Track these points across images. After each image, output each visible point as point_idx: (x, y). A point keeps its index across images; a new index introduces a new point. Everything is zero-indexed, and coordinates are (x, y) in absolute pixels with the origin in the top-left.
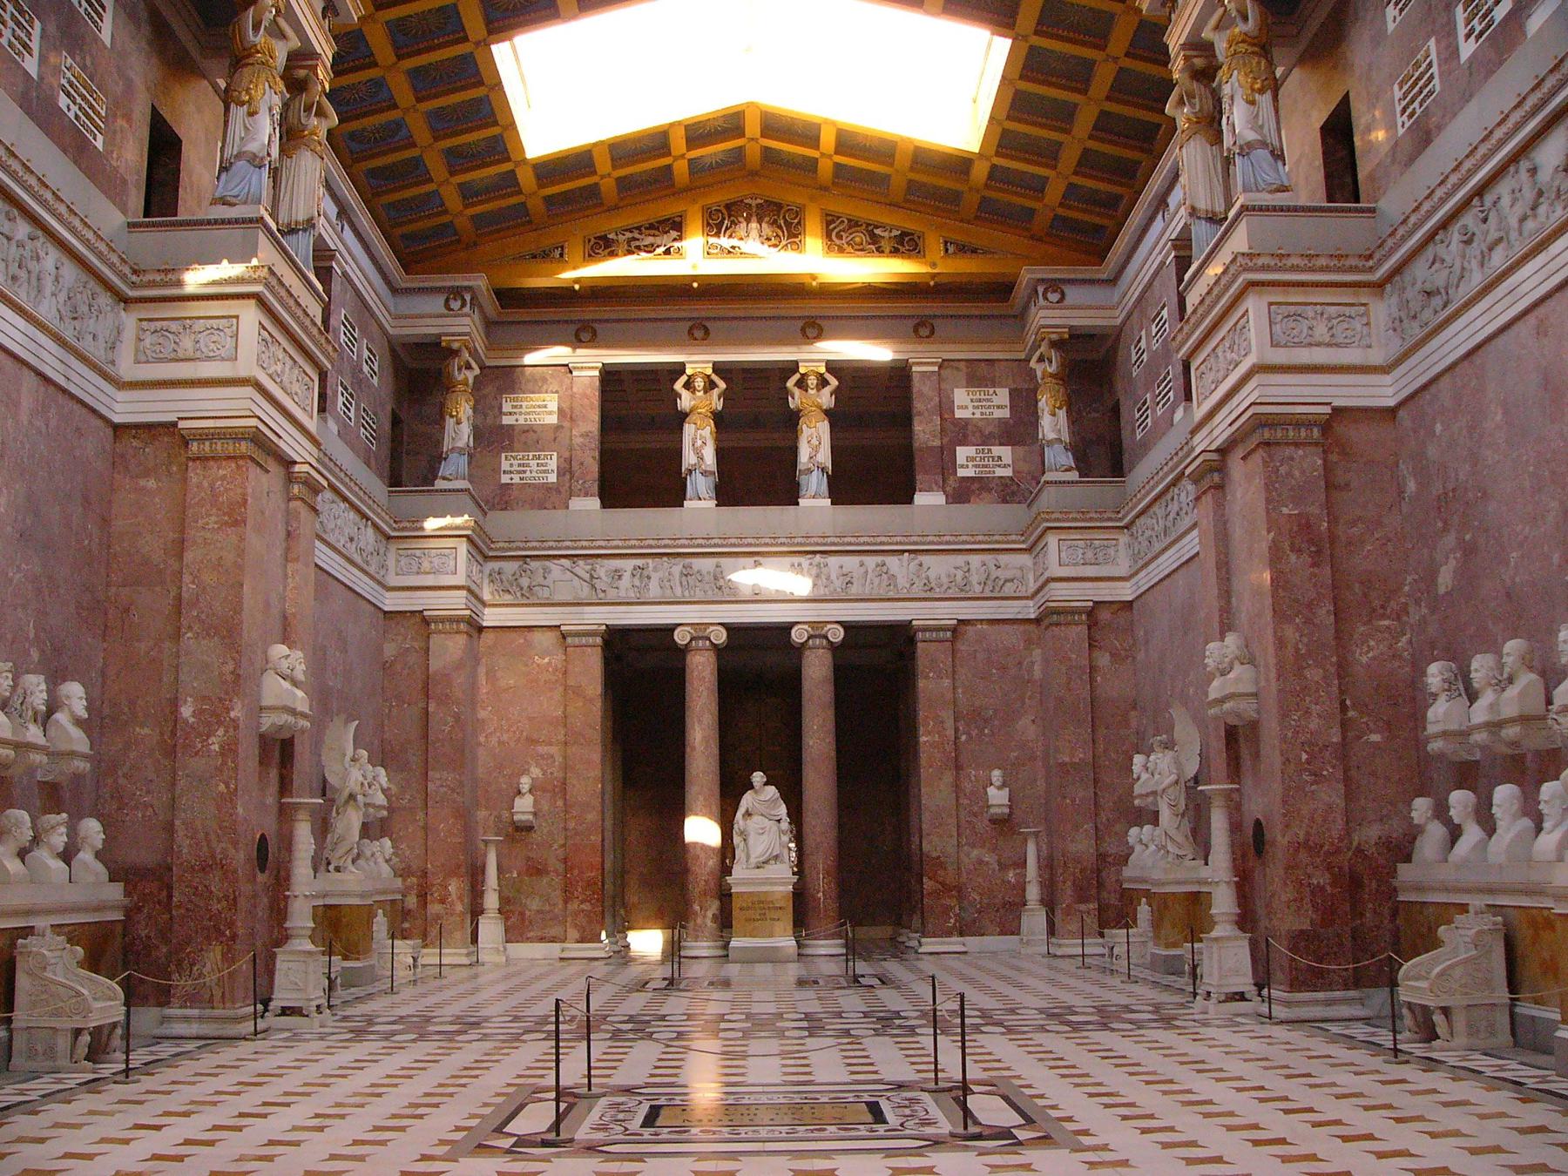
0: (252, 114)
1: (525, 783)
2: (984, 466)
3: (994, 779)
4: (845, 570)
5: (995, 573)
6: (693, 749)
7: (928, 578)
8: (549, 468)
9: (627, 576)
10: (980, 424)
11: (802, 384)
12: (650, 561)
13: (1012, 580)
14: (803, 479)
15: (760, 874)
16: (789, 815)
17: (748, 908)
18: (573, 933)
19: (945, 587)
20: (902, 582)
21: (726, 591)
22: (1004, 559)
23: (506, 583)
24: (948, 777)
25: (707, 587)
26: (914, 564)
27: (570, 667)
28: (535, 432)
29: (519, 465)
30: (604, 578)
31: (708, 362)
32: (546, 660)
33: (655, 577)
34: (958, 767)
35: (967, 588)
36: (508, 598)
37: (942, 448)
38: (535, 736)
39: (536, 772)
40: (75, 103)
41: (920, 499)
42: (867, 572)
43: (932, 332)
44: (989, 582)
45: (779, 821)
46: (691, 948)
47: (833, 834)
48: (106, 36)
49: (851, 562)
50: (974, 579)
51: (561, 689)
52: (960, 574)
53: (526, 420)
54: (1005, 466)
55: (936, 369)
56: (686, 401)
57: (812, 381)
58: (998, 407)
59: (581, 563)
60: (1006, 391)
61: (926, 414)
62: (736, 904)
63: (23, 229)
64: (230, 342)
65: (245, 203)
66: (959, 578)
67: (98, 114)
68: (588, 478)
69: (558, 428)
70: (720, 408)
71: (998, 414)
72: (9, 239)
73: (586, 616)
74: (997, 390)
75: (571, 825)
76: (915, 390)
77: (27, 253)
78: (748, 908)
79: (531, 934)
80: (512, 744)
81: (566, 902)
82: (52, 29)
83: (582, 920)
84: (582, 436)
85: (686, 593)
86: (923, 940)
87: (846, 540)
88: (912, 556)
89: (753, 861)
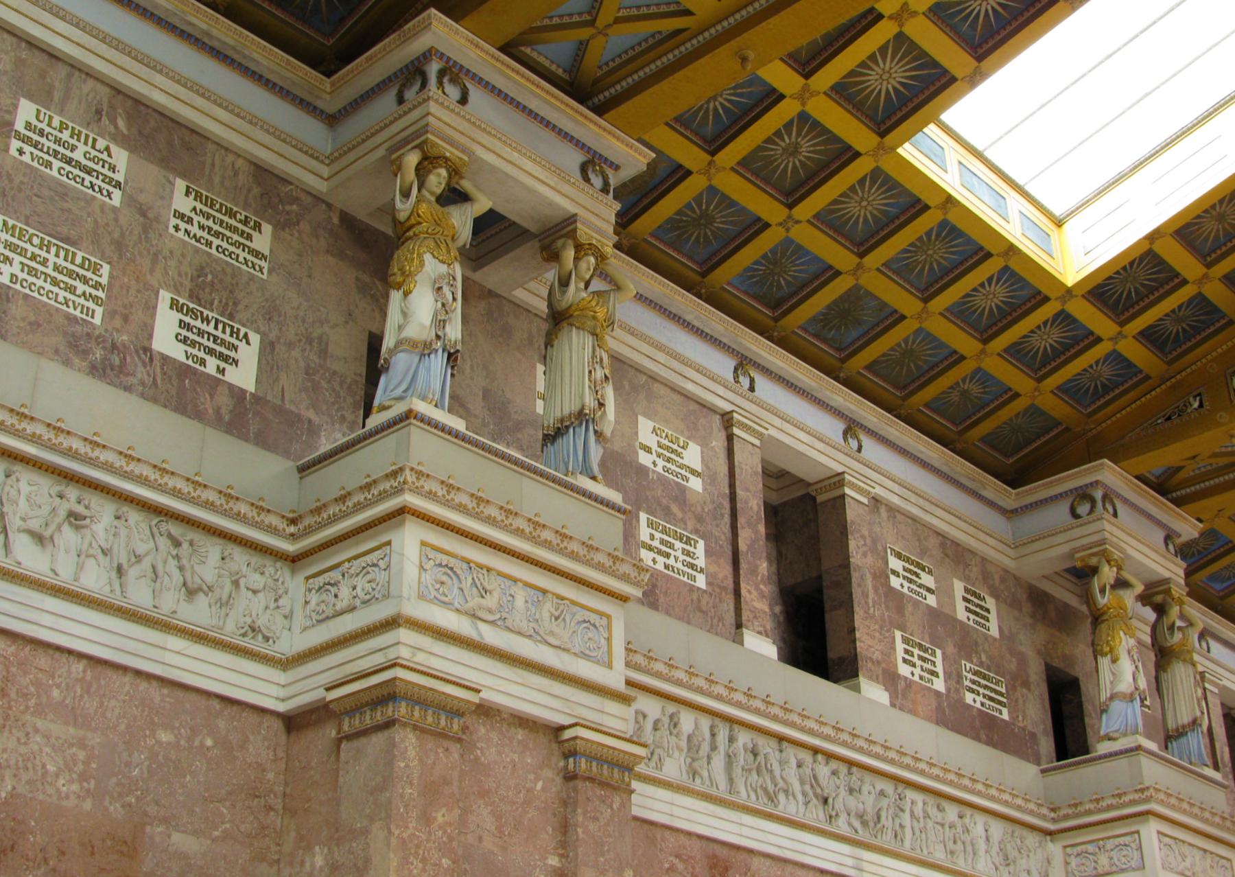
0: (1114, 661)
40: (978, 694)
48: (994, 631)
63: (952, 812)
64: (1136, 854)
65: (1125, 735)
67: (1001, 694)
72: (943, 825)
77: (959, 830)
82: (951, 649)
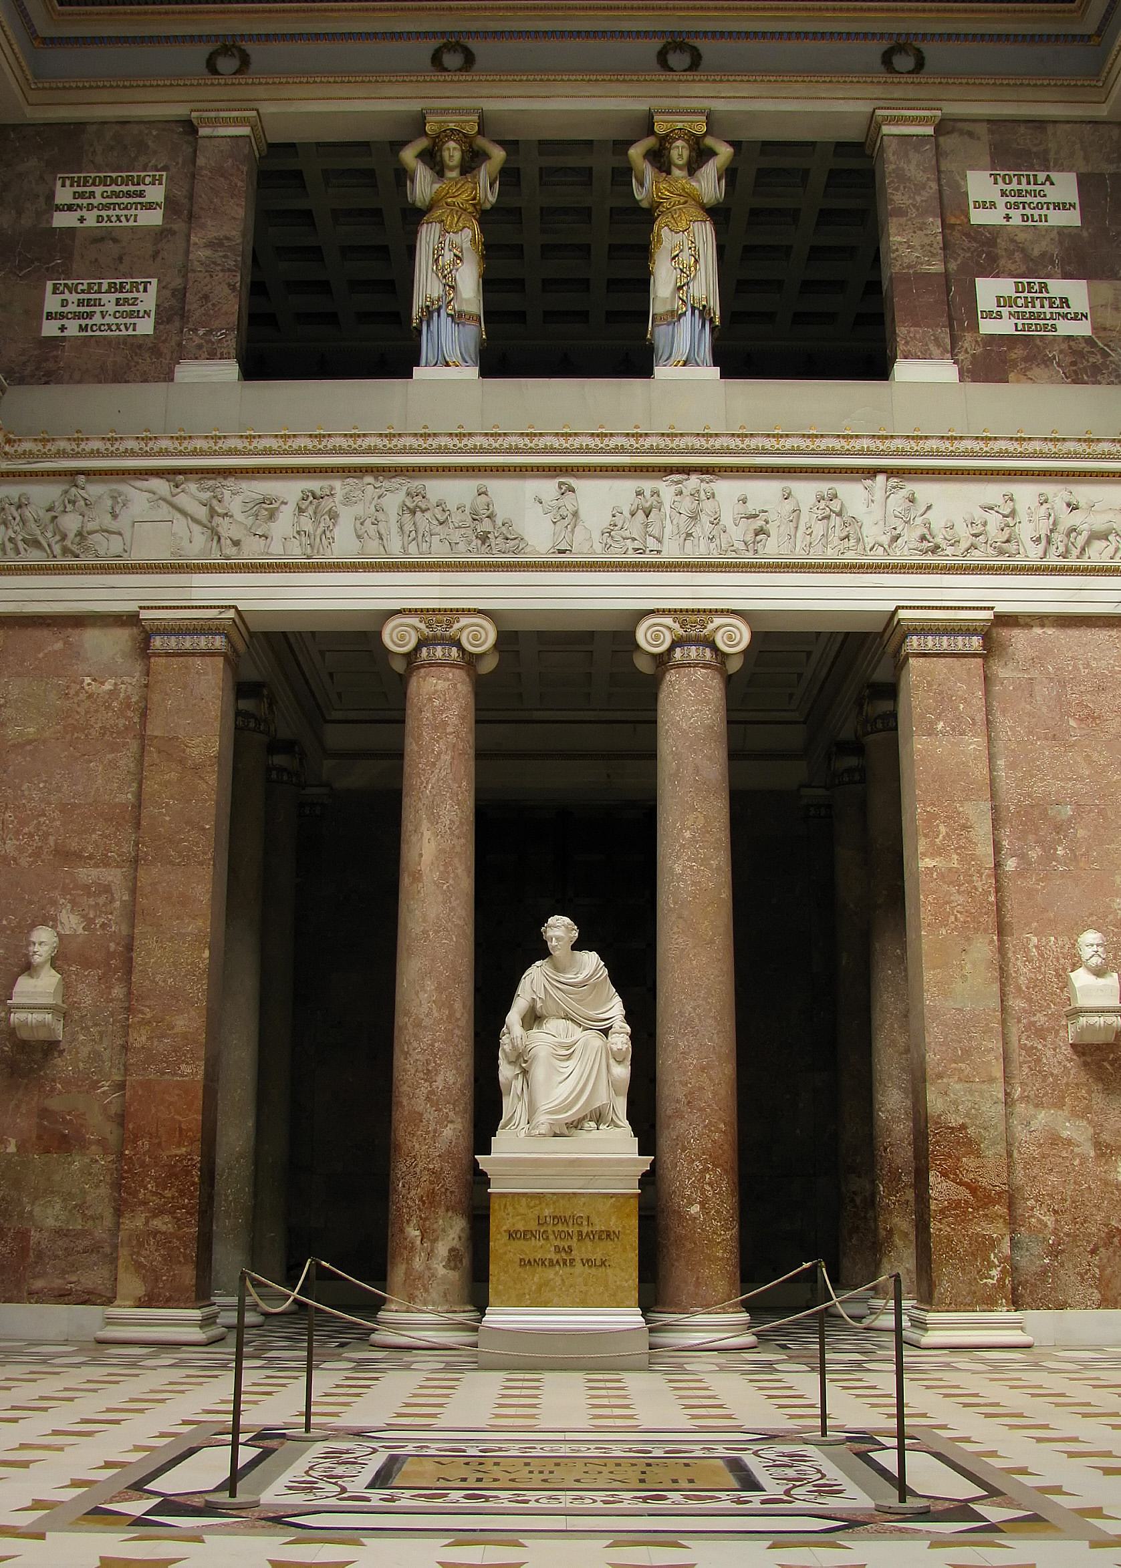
1: (43, 941)
2: (1032, 316)
3: (1086, 952)
4: (751, 508)
5: (1069, 520)
6: (417, 877)
7: (927, 525)
8: (141, 307)
9: (286, 514)
10: (1021, 237)
11: (659, 158)
12: (337, 484)
13: (1104, 536)
14: (659, 334)
15: (565, 1149)
16: (629, 1018)
17: (526, 1235)
18: (131, 1284)
19: (964, 545)
20: (873, 532)
21: (496, 542)
22: (1084, 492)
23: (32, 525)
24: (983, 948)
25: (456, 536)
26: (897, 501)
27: (156, 697)
28: (115, 241)
29: (80, 303)
30: (239, 517)
31: (468, 112)
32: (108, 686)
33: (347, 516)
34: (1002, 929)
35: (1012, 547)
36: (34, 556)
37: (946, 274)
38: (74, 845)
39: (71, 922)
41: (903, 370)
42: (797, 511)
43: (920, 65)
44: (1057, 537)
45: (605, 1032)
46: (396, 1326)
47: (726, 1070)
49: (764, 492)
50: (1025, 531)
51: (134, 746)
52: (994, 520)
53: (99, 219)
54: (1075, 318)
55: (929, 130)
56: (423, 186)
57: (679, 152)
58: (1057, 206)
59: (192, 487)
60: (1072, 177)
61: (913, 213)
62: (501, 1223)
66: (992, 529)
68: (216, 324)
69: (161, 234)
70: (492, 199)
71: (1057, 219)
73: (196, 594)
74: (1054, 176)
75: (140, 1038)
76: (890, 168)
78: (526, 1235)
79: (39, 1284)
80: (24, 861)
81: (118, 1213)
83: (152, 1255)
84: (210, 245)
85: (413, 548)
86: (931, 1316)
87: (754, 443)
88: (893, 481)
89: (543, 1120)
